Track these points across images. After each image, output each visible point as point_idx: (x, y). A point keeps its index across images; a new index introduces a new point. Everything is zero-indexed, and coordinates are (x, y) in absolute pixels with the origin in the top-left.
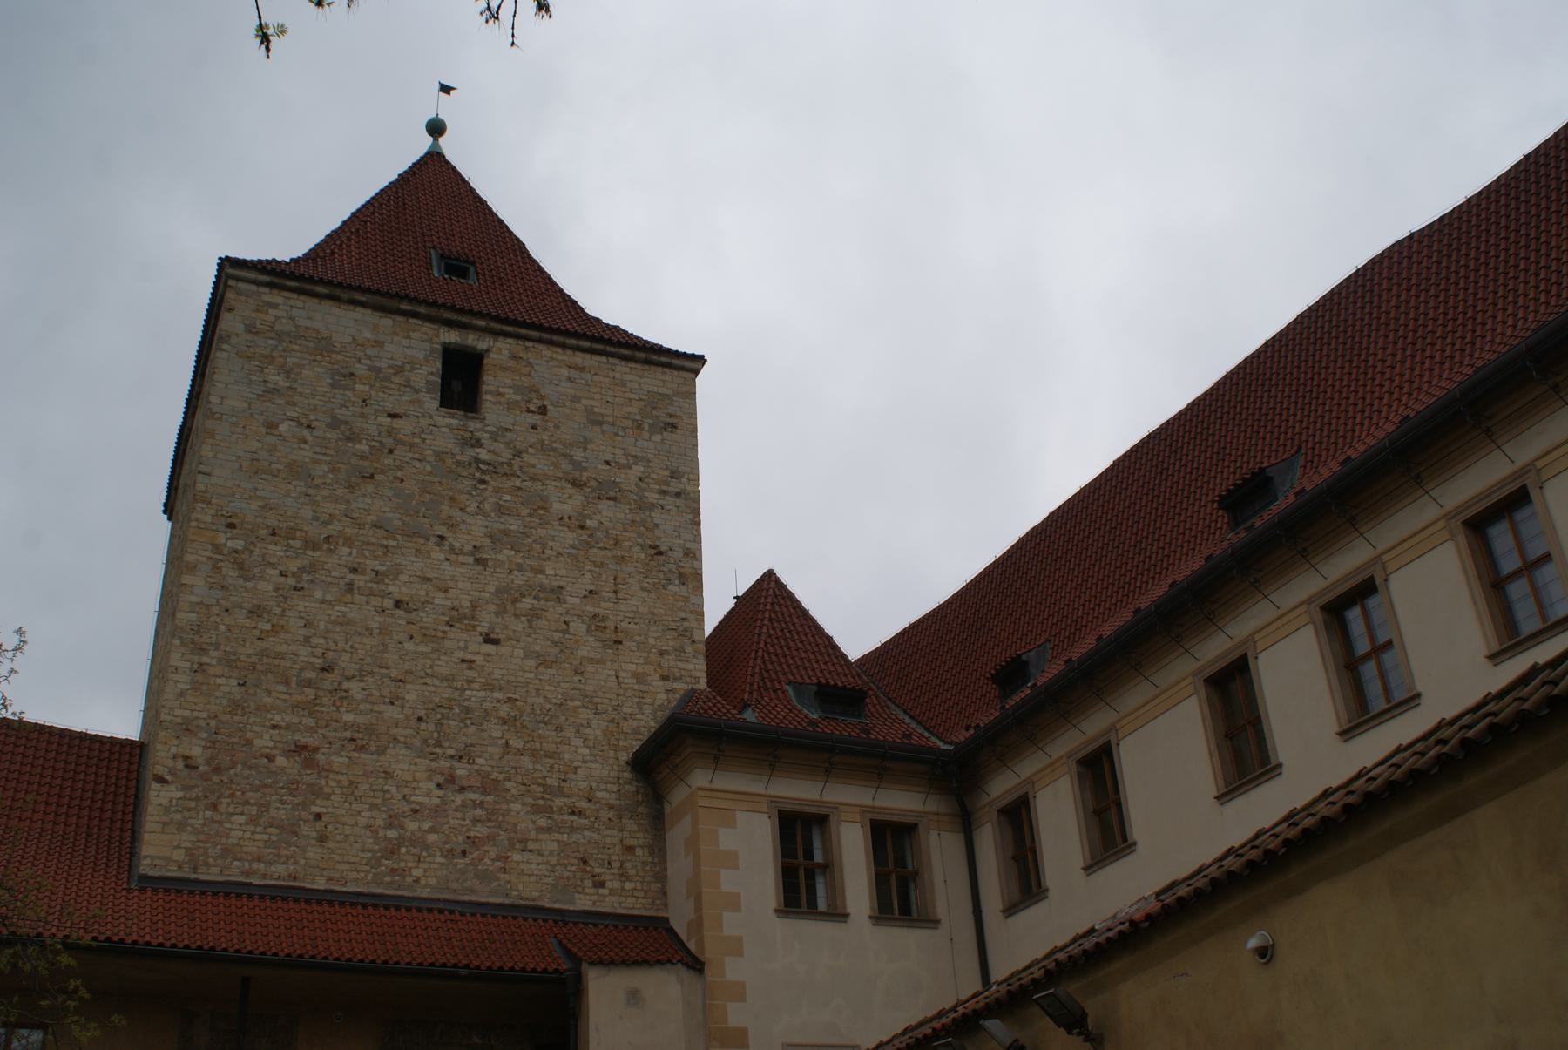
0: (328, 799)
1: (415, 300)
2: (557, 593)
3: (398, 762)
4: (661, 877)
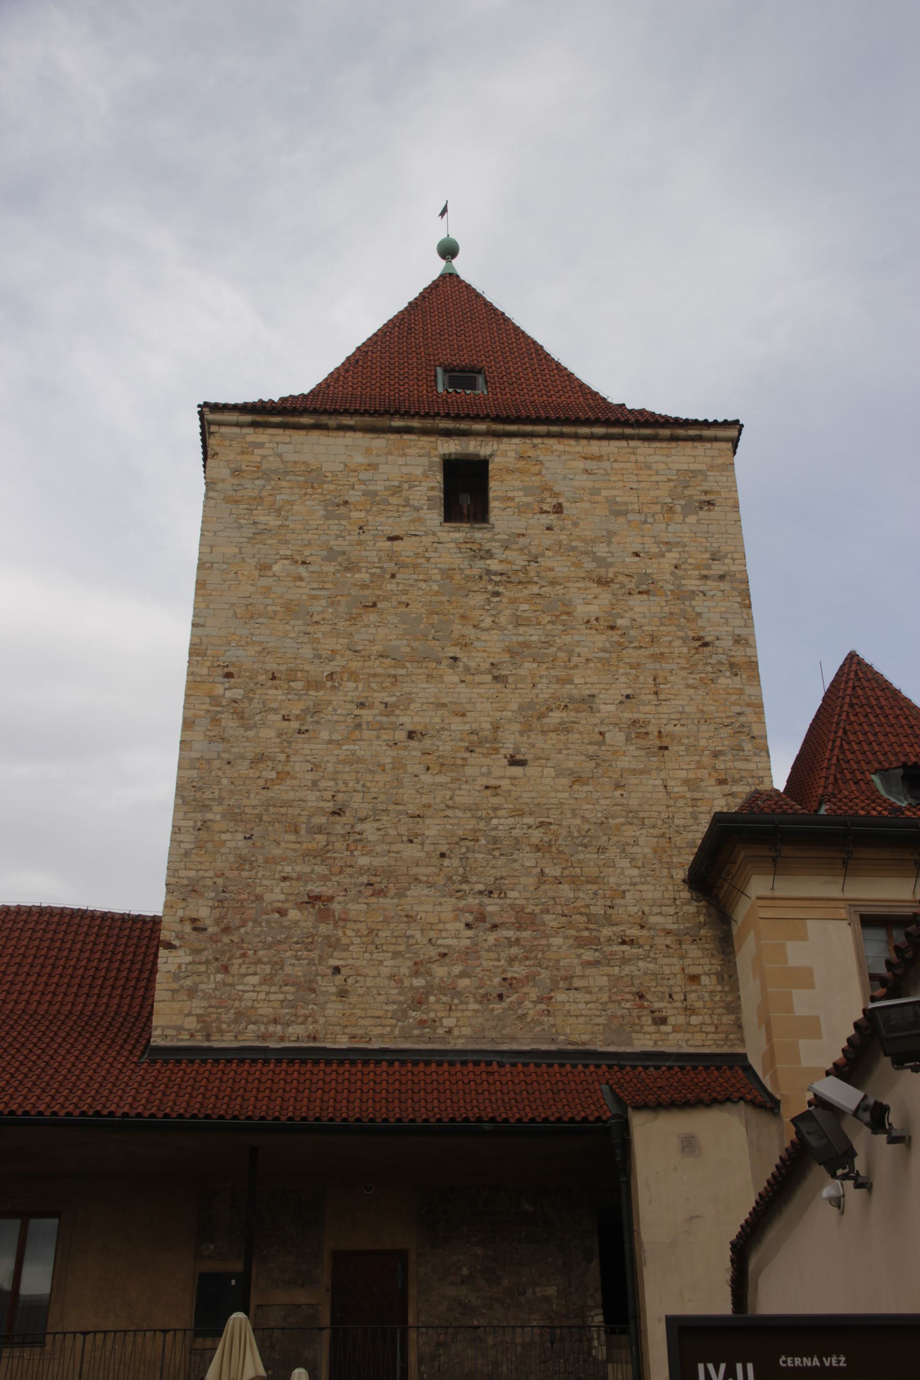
0: (346, 950)
1: (406, 414)
2: (588, 702)
3: (421, 903)
4: (734, 1008)
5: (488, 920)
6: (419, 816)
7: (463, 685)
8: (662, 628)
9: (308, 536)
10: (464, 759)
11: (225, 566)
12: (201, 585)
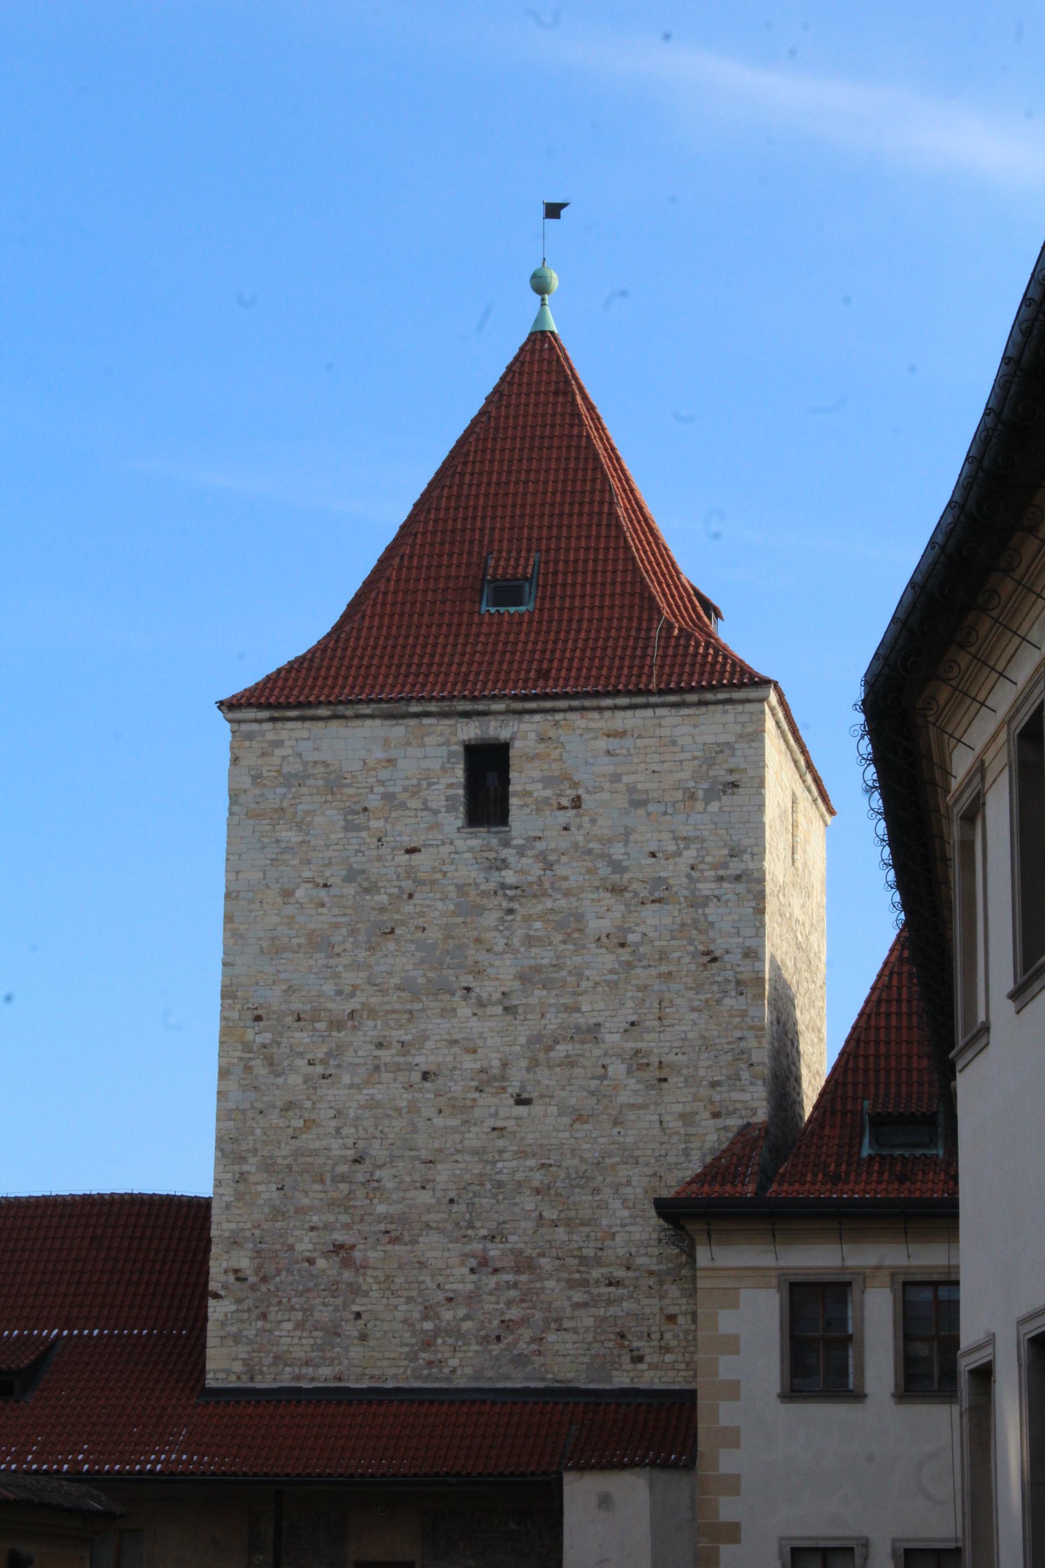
0: (365, 1296)
2: (593, 1032)
5: (490, 1264)
6: (431, 1162)
7: (475, 1018)
8: (673, 943)
9: (328, 854)
10: (474, 1100)
11: (251, 894)
12: (228, 918)
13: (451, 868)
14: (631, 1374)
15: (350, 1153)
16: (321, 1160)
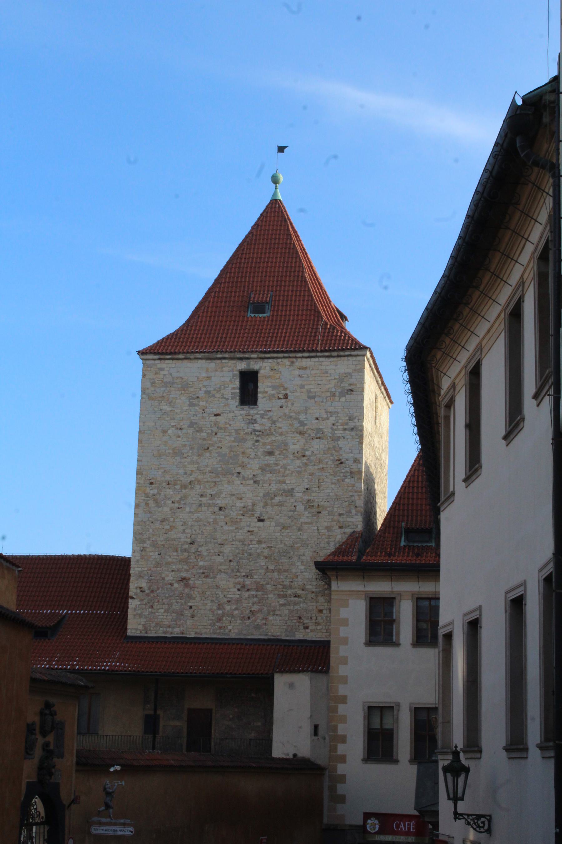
2: (290, 492)
8: (325, 455)
9: (182, 416)
10: (241, 519)
11: (149, 432)
12: (140, 441)
13: (233, 422)
14: (304, 634)
15: (189, 540)
16: (177, 543)
